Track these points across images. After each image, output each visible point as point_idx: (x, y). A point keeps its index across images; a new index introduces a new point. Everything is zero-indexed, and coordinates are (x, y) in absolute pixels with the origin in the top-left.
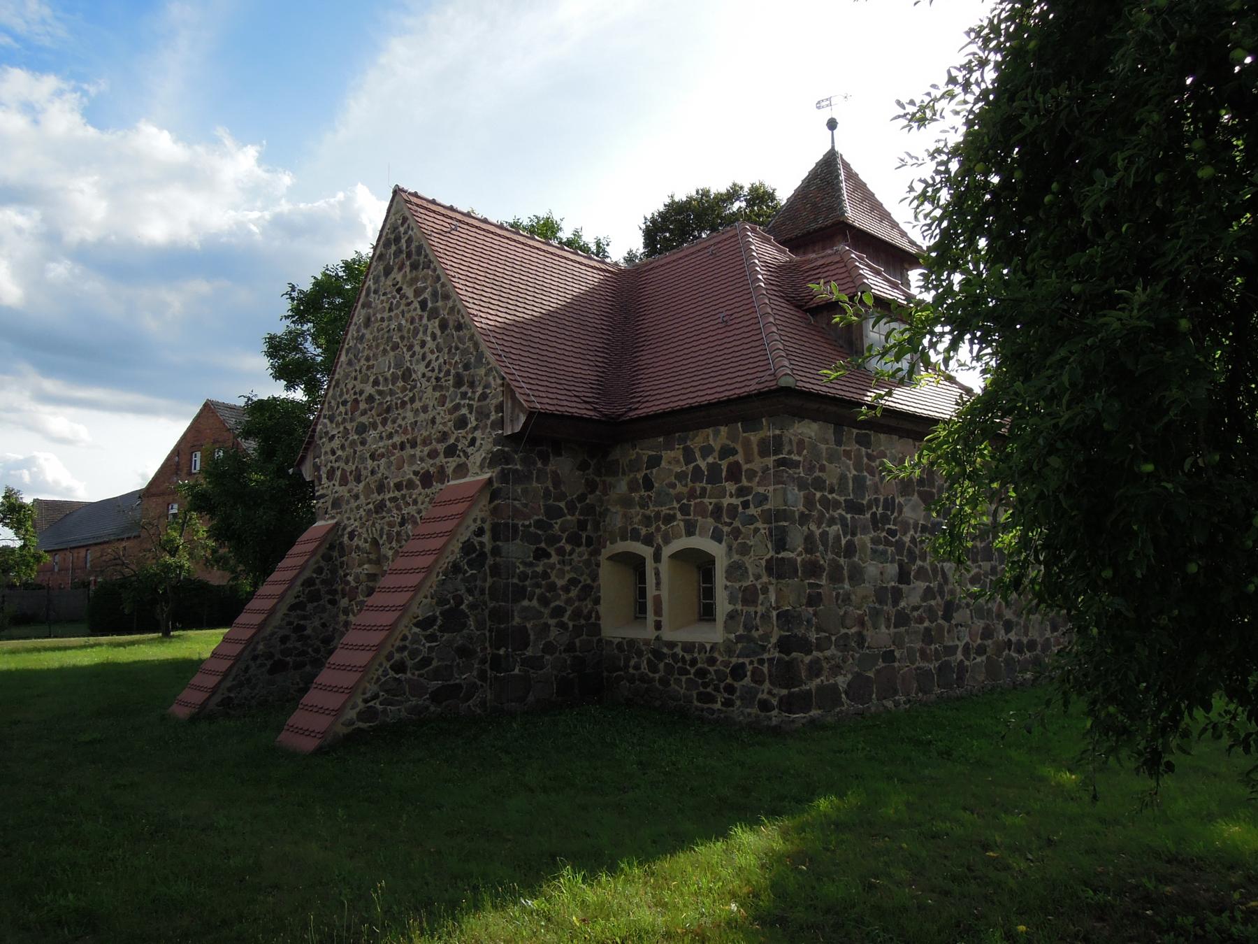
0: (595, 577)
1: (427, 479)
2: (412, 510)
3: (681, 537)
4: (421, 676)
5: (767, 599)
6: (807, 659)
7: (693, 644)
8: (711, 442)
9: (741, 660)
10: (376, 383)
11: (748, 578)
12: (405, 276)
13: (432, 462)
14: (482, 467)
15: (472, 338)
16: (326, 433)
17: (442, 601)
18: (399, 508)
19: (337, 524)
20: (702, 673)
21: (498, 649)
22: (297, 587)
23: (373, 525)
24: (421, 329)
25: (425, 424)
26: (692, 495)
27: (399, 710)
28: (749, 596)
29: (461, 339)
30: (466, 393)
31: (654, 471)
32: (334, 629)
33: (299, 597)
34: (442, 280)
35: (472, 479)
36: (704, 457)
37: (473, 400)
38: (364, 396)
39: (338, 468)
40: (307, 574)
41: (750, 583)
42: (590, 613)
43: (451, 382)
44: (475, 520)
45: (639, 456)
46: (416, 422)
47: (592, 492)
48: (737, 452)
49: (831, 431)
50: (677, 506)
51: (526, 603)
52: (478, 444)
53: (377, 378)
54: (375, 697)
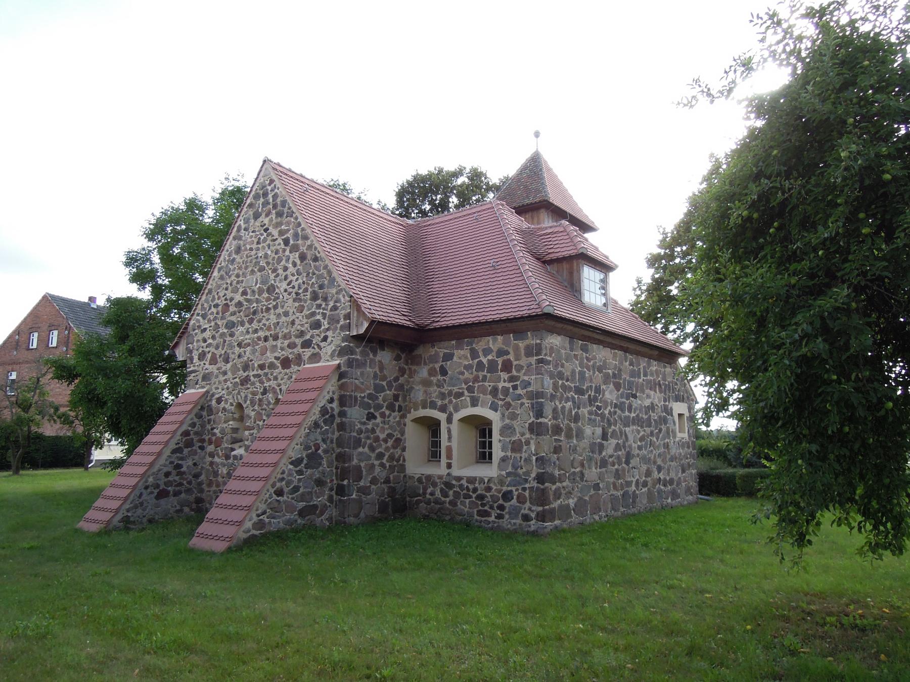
0: (403, 433)
1: (286, 363)
2: (273, 383)
3: (468, 407)
4: (293, 498)
5: (529, 449)
6: (554, 487)
7: (475, 478)
8: (491, 346)
9: (509, 488)
10: (244, 293)
11: (516, 434)
12: (271, 220)
13: (291, 351)
14: (332, 356)
15: (326, 267)
16: (199, 327)
17: (307, 448)
18: (262, 382)
19: (207, 392)
20: (481, 497)
21: (343, 480)
22: (178, 437)
23: (239, 393)
24: (284, 258)
25: (286, 324)
26: (476, 380)
27: (279, 522)
28: (516, 447)
29: (317, 268)
30: (321, 305)
31: (448, 363)
32: (202, 467)
33: (178, 443)
34: (302, 226)
35: (324, 364)
36: (485, 355)
37: (327, 310)
38: (233, 302)
39: (209, 352)
40: (185, 427)
41: (517, 438)
42: (400, 457)
43: (308, 297)
44: (328, 392)
45: (437, 354)
46: (278, 323)
47: (402, 376)
48: (509, 353)
49: (568, 342)
50: (465, 387)
51: (361, 449)
52: (329, 340)
53: (246, 290)
54: (264, 513)
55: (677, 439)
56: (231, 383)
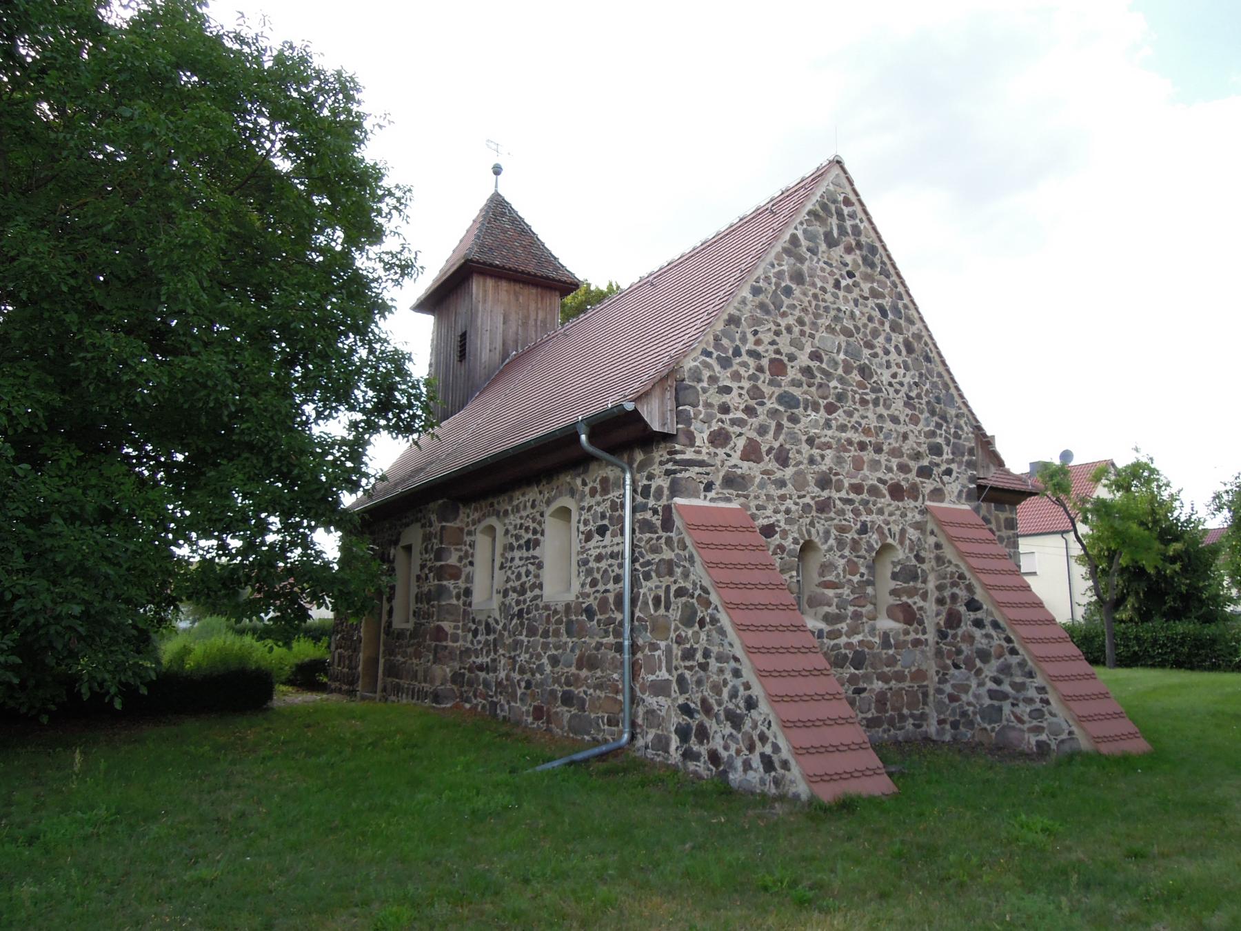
1: (897, 492)
2: (879, 520)
10: (815, 356)
18: (856, 512)
23: (812, 524)
39: (741, 434)
46: (881, 428)
52: (954, 474)
56: (796, 504)
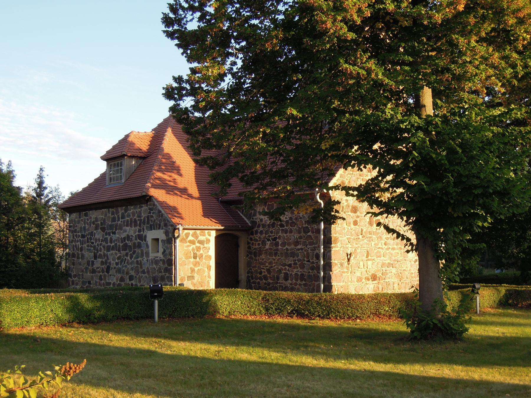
55: (150, 258)
